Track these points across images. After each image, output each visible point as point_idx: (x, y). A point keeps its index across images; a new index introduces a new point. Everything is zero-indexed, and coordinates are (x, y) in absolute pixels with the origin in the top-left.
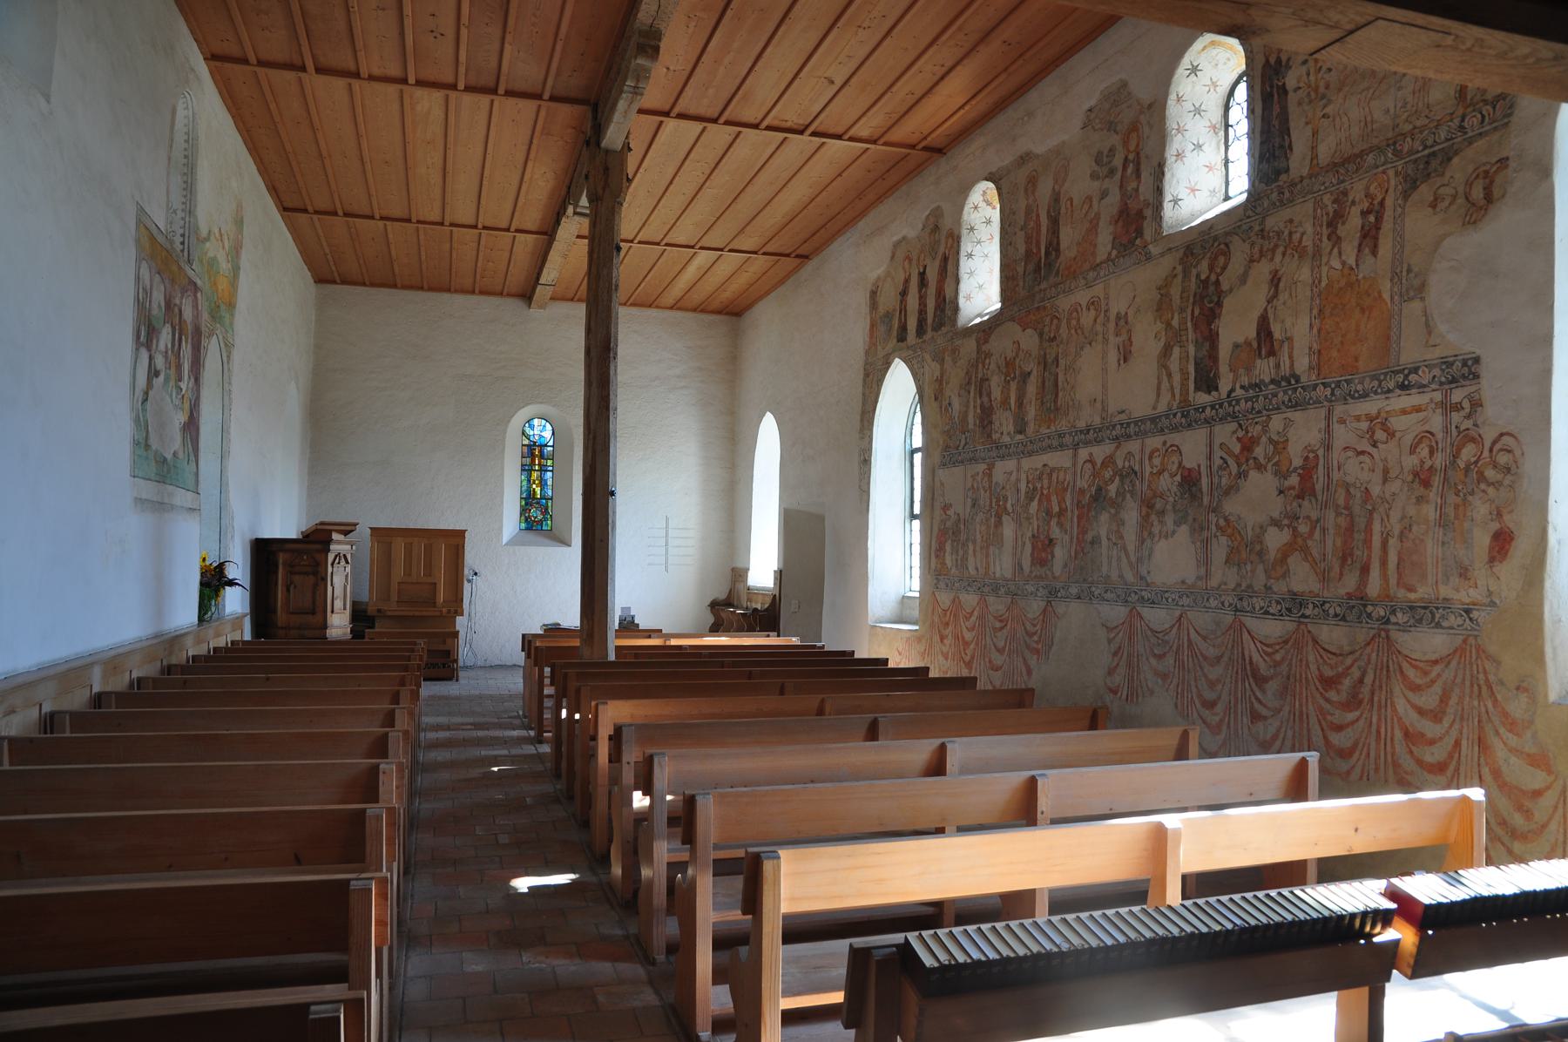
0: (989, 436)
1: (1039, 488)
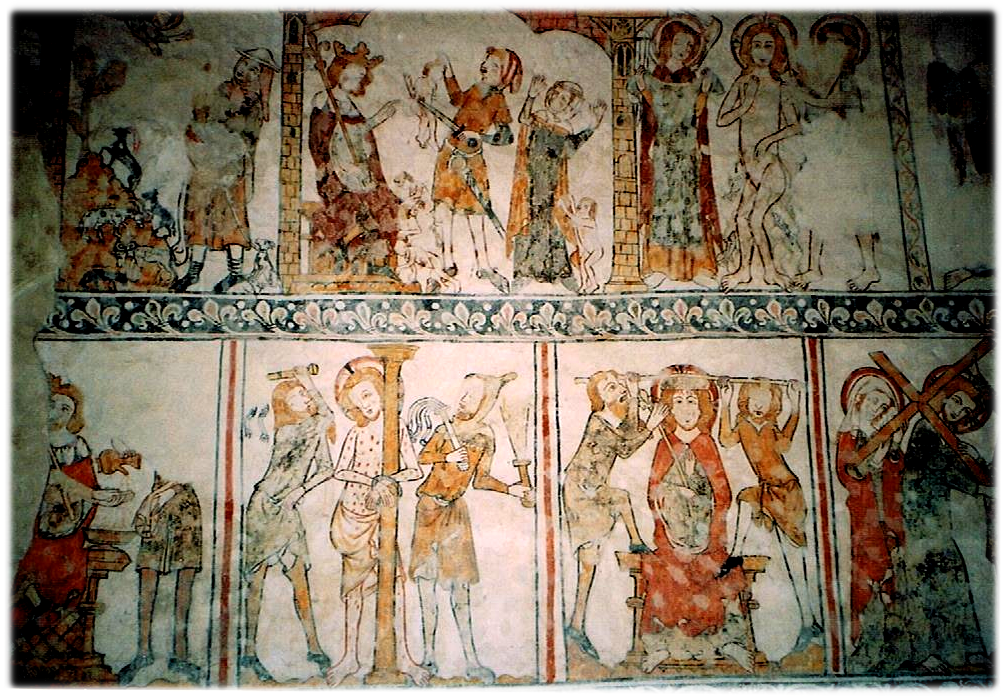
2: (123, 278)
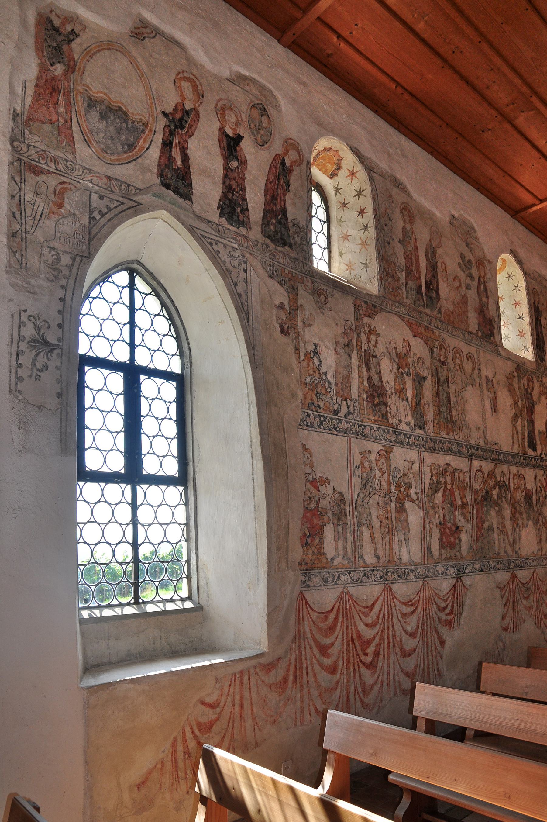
0: (385, 416)
1: (443, 482)
2: (319, 407)
